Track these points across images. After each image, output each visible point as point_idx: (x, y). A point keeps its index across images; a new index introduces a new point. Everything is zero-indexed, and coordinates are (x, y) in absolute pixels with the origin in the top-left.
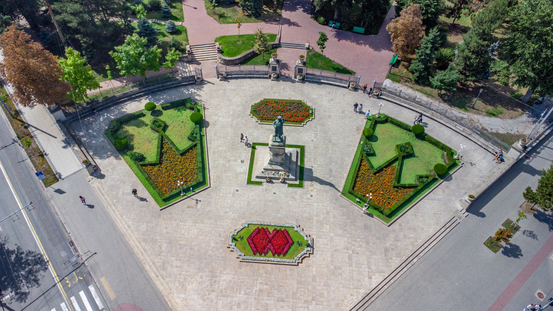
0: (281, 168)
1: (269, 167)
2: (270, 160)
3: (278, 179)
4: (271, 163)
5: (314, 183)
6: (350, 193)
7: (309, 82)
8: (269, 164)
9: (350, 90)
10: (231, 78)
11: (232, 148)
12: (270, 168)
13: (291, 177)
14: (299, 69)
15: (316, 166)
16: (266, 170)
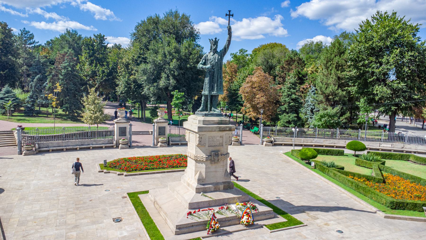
0: (230, 195)
1: (201, 198)
2: (199, 180)
3: (236, 220)
4: (203, 186)
5: (312, 213)
6: (397, 206)
7: (177, 145)
8: (198, 191)
9: (234, 145)
10: (48, 151)
11: (77, 209)
12: (206, 199)
13: (262, 209)
14: (160, 128)
15: (282, 195)
16: (195, 207)
